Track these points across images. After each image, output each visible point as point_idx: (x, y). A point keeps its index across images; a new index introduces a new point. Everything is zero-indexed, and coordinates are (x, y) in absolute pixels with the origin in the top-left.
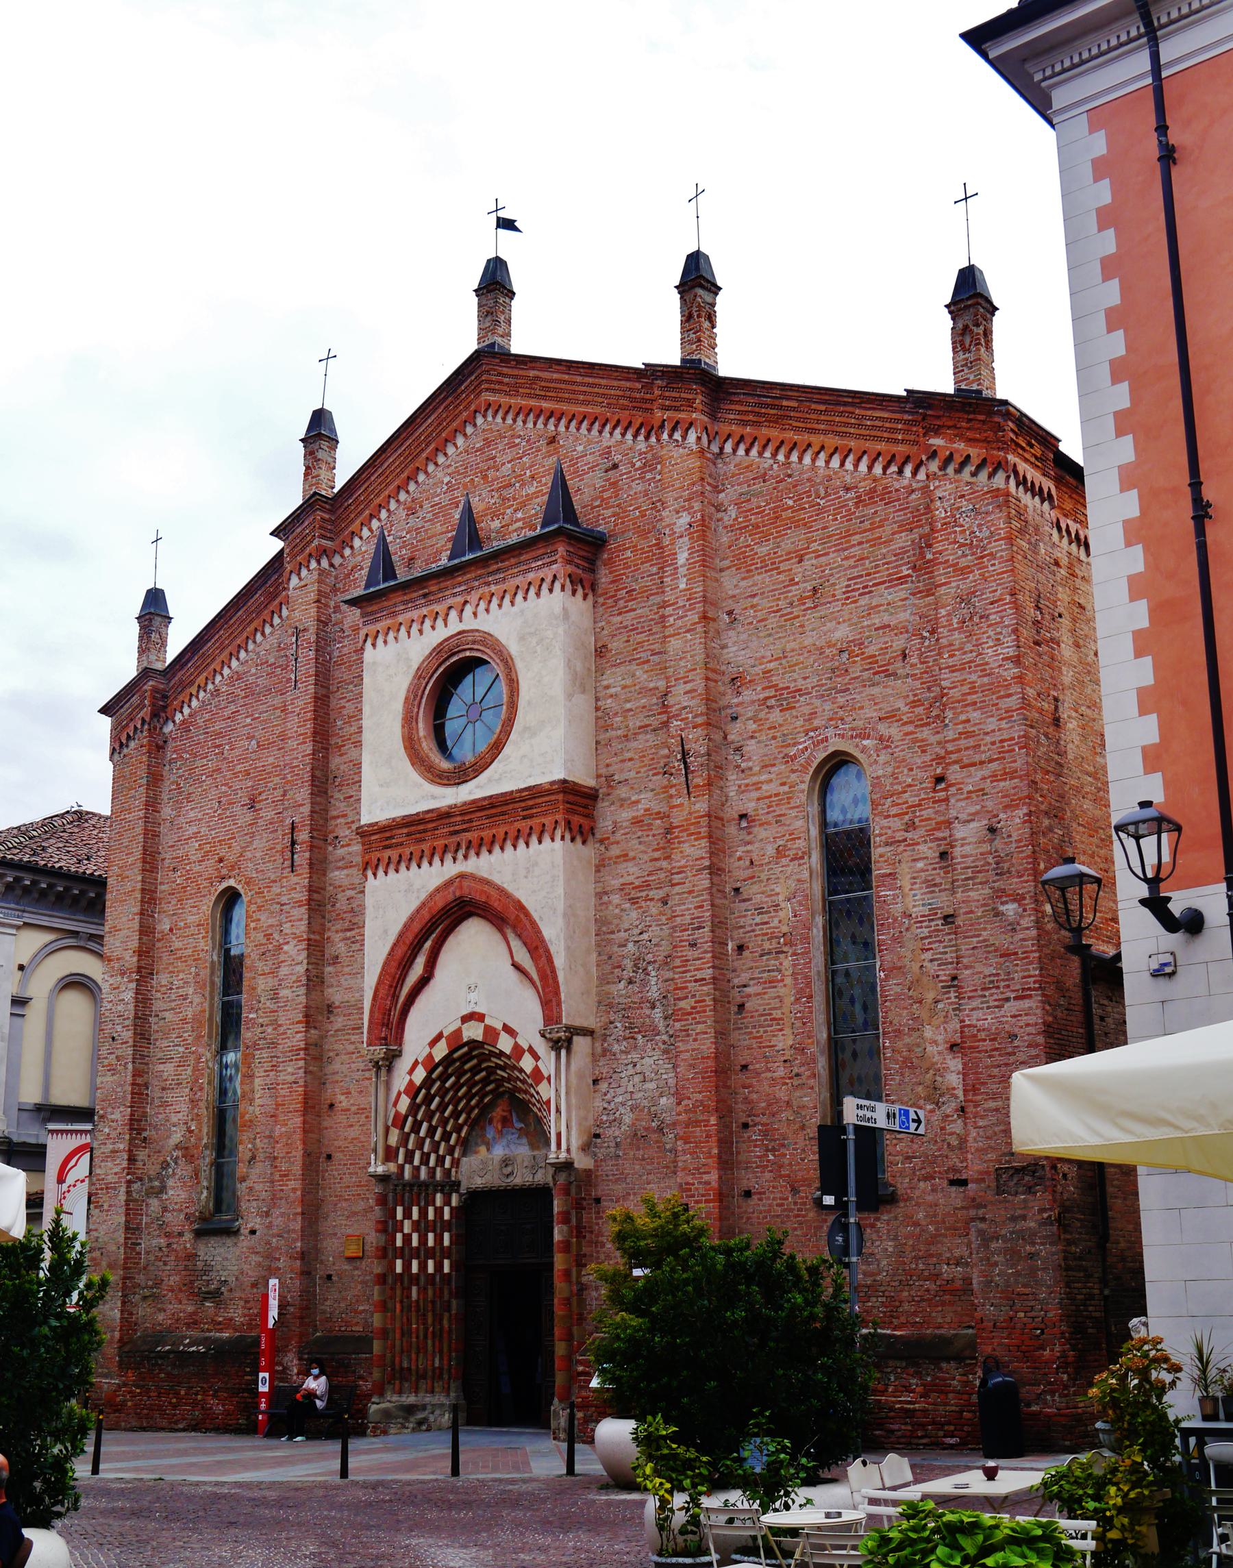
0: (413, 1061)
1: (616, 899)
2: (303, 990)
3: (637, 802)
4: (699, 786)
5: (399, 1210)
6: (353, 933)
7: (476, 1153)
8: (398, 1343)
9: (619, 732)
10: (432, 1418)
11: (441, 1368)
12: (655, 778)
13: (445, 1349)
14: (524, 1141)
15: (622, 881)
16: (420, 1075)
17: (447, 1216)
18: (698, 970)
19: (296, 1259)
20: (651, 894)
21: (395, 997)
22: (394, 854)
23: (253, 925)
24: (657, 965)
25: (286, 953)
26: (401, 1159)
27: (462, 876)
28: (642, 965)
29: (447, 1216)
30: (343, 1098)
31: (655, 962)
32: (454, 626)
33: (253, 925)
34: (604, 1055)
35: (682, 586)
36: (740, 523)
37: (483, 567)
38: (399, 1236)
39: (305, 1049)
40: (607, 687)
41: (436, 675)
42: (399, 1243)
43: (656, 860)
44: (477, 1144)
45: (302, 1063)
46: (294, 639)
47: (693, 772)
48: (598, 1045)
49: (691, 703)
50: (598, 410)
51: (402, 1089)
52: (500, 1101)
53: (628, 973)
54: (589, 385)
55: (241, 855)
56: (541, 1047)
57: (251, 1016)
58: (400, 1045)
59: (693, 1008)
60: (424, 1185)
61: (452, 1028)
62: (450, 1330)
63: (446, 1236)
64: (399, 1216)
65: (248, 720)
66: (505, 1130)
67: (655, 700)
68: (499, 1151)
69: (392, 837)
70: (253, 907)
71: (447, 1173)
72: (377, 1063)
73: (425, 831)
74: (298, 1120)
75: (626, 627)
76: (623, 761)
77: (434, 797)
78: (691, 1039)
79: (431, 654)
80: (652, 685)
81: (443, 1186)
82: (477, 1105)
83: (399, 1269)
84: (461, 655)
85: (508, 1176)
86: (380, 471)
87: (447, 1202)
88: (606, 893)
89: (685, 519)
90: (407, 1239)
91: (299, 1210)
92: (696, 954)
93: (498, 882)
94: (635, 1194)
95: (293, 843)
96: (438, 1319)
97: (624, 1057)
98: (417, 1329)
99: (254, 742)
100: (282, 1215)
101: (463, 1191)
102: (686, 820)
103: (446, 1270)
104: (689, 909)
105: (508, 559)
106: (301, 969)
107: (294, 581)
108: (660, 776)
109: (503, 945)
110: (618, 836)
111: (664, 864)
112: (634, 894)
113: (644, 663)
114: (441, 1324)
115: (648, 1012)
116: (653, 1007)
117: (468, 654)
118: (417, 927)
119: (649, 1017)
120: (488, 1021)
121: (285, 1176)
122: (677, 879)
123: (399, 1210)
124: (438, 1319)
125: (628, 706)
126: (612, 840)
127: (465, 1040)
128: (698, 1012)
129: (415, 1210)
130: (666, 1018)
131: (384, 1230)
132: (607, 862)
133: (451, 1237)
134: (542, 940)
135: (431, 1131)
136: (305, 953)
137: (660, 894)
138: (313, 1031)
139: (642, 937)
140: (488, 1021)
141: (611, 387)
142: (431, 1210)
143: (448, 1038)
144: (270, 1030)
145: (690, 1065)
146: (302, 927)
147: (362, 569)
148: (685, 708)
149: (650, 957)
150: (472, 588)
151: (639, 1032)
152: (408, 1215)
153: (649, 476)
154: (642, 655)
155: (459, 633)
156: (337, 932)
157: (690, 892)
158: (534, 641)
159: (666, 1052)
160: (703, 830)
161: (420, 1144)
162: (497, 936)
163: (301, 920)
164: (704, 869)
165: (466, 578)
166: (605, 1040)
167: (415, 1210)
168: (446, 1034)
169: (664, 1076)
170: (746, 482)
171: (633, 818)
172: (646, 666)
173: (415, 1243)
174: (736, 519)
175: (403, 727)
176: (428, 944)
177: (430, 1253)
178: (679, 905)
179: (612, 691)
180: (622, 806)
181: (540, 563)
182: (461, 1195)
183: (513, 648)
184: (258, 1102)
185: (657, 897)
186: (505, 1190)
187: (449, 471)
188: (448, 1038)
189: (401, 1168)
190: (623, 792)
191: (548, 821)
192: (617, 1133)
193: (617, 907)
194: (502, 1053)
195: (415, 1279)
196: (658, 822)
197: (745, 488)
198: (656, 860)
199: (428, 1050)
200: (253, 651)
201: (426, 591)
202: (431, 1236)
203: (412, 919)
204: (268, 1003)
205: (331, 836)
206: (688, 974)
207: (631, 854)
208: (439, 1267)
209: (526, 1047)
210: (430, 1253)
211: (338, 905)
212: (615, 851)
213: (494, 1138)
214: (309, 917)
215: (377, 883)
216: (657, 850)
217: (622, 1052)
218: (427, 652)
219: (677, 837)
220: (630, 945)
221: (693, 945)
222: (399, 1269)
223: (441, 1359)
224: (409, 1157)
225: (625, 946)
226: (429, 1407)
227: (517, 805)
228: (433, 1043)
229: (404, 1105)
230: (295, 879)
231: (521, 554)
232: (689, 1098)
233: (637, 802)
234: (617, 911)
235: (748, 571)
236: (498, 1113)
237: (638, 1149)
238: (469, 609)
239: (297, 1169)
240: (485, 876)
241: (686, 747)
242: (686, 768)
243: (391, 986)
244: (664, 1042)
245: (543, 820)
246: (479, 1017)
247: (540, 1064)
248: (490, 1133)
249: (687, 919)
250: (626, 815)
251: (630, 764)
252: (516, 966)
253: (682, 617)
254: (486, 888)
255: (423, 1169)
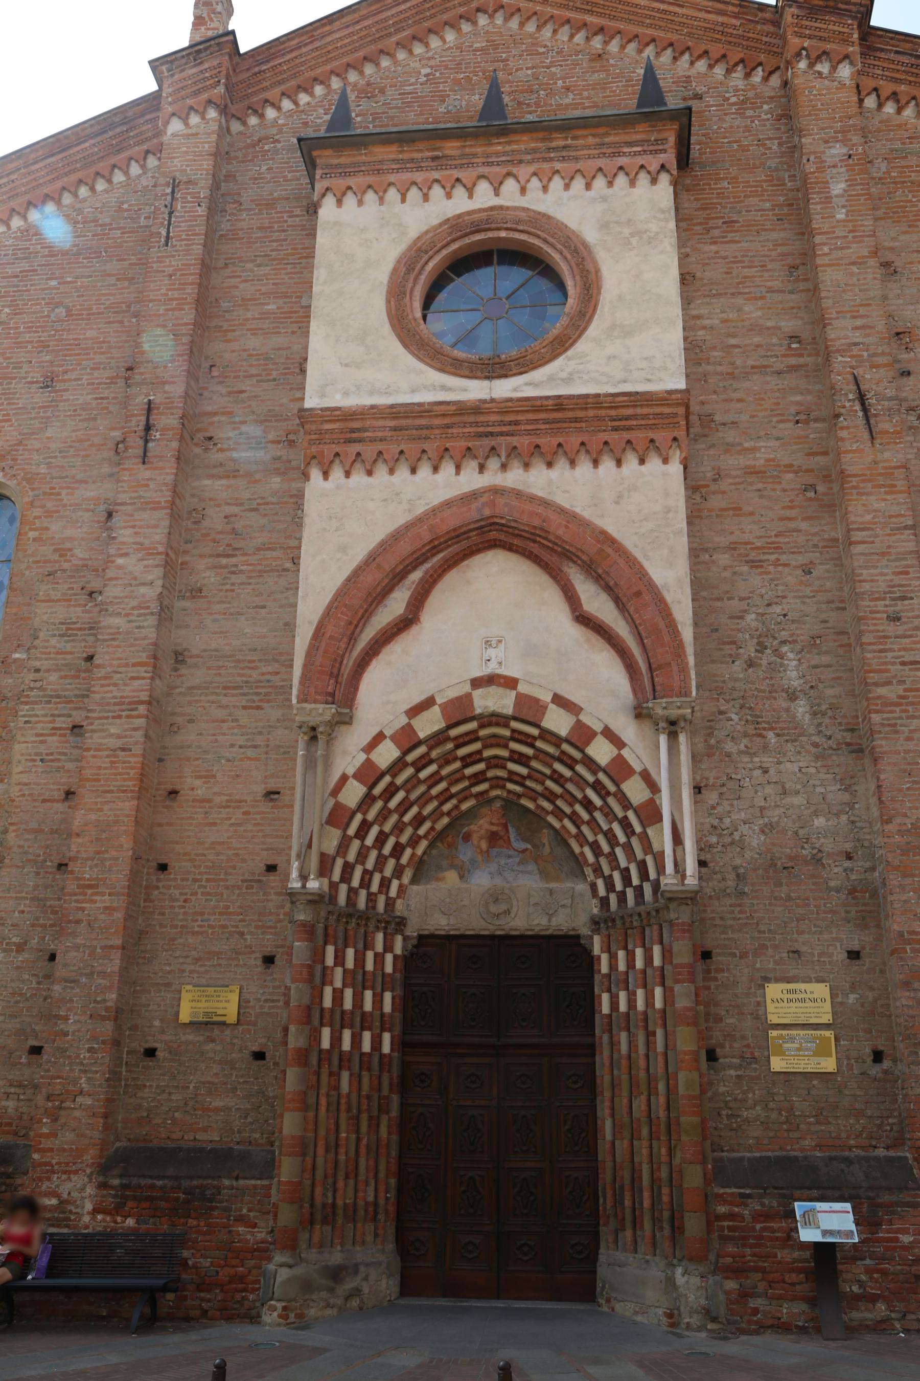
0: (374, 731)
1: (724, 559)
2: (152, 621)
3: (754, 449)
4: (887, 432)
5: (330, 950)
6: (233, 560)
7: (439, 880)
8: (320, 1161)
9: (719, 369)
10: (366, 1290)
11: (376, 1204)
12: (781, 426)
13: (382, 1175)
14: (532, 867)
15: (733, 538)
16: (386, 754)
17: (389, 969)
18: (905, 649)
19: (103, 1018)
20: (784, 558)
21: (352, 639)
22: (369, 451)
23: (32, 534)
24: (798, 647)
25: (120, 567)
26: (336, 876)
27: (496, 491)
28: (768, 642)
29: (389, 969)
30: (198, 782)
31: (795, 642)
32: (484, 197)
33: (32, 534)
34: (709, 755)
35: (841, 216)
36: (891, 178)
37: (543, 140)
38: (328, 991)
39: (149, 703)
40: (698, 317)
41: (445, 252)
42: (328, 1002)
43: (790, 519)
44: (440, 868)
45: (141, 722)
46: (169, 190)
47: (876, 415)
48: (699, 739)
49: (867, 340)
50: (674, 37)
51: (351, 771)
52: (485, 810)
53: (750, 650)
54: (665, 12)
55: (20, 443)
56: (628, 730)
57: (17, 656)
58: (351, 707)
59: (900, 697)
60: (364, 917)
61: (452, 694)
62: (388, 1145)
63: (388, 996)
64: (330, 961)
65: (54, 283)
66: (495, 851)
67: (775, 340)
68: (482, 880)
69: (365, 430)
70: (37, 512)
71: (390, 903)
72: (314, 729)
73: (428, 428)
74: (127, 806)
75: (725, 258)
76: (726, 401)
77: (444, 388)
78: (902, 737)
79: (440, 225)
80: (769, 324)
81: (387, 922)
82: (449, 813)
83: (326, 1044)
84: (490, 235)
85: (498, 916)
86: (318, 44)
87: (388, 948)
88: (706, 550)
89: (838, 150)
90: (338, 996)
91: (118, 942)
92: (900, 629)
93: (566, 504)
94: (775, 947)
95: (148, 428)
96: (374, 1124)
97: (746, 759)
98: (347, 1139)
99: (61, 311)
100: (77, 947)
101: (411, 931)
102: (869, 469)
103: (386, 1049)
104: (882, 574)
105: (586, 136)
106: (150, 593)
107: (176, 126)
108: (791, 425)
109: (553, 595)
110: (724, 485)
111: (804, 526)
112: (753, 555)
113: (756, 299)
114: (377, 1132)
115: (784, 705)
116: (792, 696)
117: (503, 234)
118: (406, 548)
119: (787, 710)
120: (522, 688)
121: (90, 887)
122: (857, 536)
123: (330, 950)
124: (374, 1124)
125: (733, 341)
126: (713, 487)
127: (478, 711)
128: (912, 704)
129: (350, 953)
130: (814, 714)
131: (310, 980)
132: (705, 513)
133: (393, 998)
134: (651, 585)
135: (381, 839)
136: (160, 572)
137: (801, 559)
138: (158, 681)
139: (770, 610)
140: (522, 688)
141: (695, 18)
142: (370, 955)
143: (444, 707)
144: (54, 677)
145: (905, 771)
146: (158, 537)
147: (277, 141)
148: (856, 344)
149: (784, 635)
150: (521, 162)
151: (772, 729)
152: (340, 959)
153: (749, 113)
154: (752, 289)
155: (492, 208)
156: (201, 556)
157: (883, 554)
158: (626, 231)
159: (817, 757)
160: (899, 483)
161: (362, 856)
162: (543, 578)
163: (156, 526)
164: (906, 528)
165: (508, 148)
166: (710, 735)
167: (350, 953)
168: (439, 700)
169: (822, 790)
170: (901, 139)
171: (747, 467)
172: (760, 303)
173: (348, 1004)
174: (888, 172)
175: (388, 301)
176: (416, 575)
177: (365, 1022)
178: (867, 568)
179: (707, 322)
180: (727, 451)
181: (639, 149)
182: (405, 939)
183: (591, 235)
184: (16, 778)
185: (793, 563)
186: (493, 937)
187: (432, 63)
188: (444, 707)
189: (334, 886)
190: (730, 435)
191: (661, 436)
192: (738, 861)
193: (725, 568)
194: (547, 735)
195: (344, 1060)
196: (791, 476)
197: (898, 145)
198: (790, 519)
199: (404, 720)
200: (72, 206)
201: (440, 154)
202: (368, 994)
203: (396, 537)
204: (53, 641)
205: (200, 436)
206: (890, 655)
207: (747, 509)
208: (377, 1043)
209: (598, 727)
210: (365, 1022)
211: (207, 523)
212: (717, 502)
213: (473, 861)
214: (171, 527)
215: (329, 485)
216: (791, 508)
217: (740, 752)
218: (435, 222)
219: (854, 487)
220: (750, 618)
221: (895, 618)
222: (326, 1044)
223: (376, 1190)
224: (348, 869)
225: (742, 618)
226: (362, 1269)
227: (603, 412)
228: (416, 710)
229: (353, 793)
230: (148, 474)
231: (607, 134)
232: (905, 815)
233: (754, 449)
234: (727, 574)
235: (910, 226)
236: (482, 825)
237: (779, 884)
238: (510, 185)
239: (119, 876)
240: (540, 494)
241: (862, 387)
242: (865, 410)
243: (350, 623)
244: (816, 745)
245: (651, 435)
246: (511, 683)
247: (625, 752)
248: (466, 853)
249: (882, 587)
250: (734, 462)
251: (739, 405)
252: (584, 619)
253: (842, 248)
254: (540, 510)
255: (363, 893)
